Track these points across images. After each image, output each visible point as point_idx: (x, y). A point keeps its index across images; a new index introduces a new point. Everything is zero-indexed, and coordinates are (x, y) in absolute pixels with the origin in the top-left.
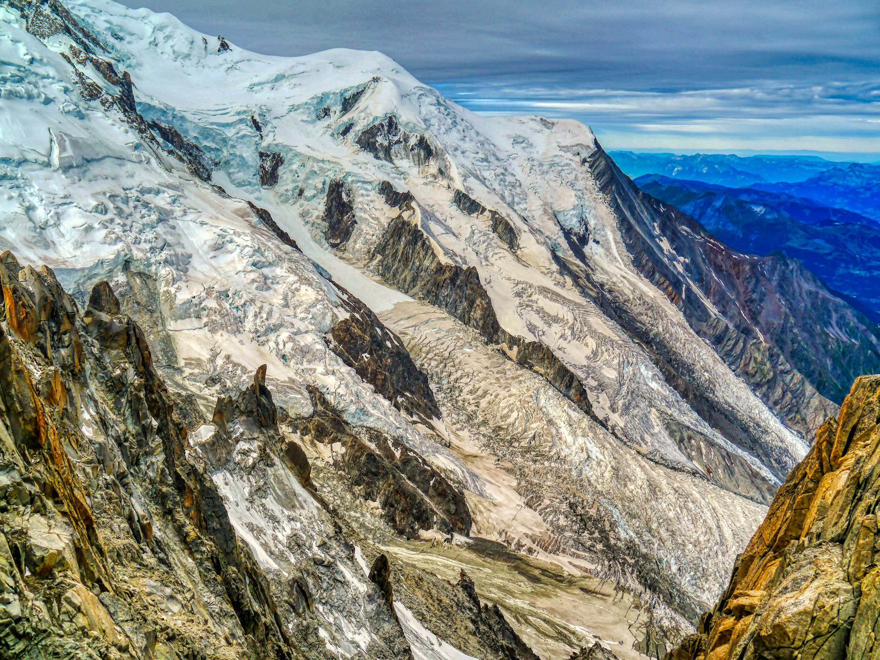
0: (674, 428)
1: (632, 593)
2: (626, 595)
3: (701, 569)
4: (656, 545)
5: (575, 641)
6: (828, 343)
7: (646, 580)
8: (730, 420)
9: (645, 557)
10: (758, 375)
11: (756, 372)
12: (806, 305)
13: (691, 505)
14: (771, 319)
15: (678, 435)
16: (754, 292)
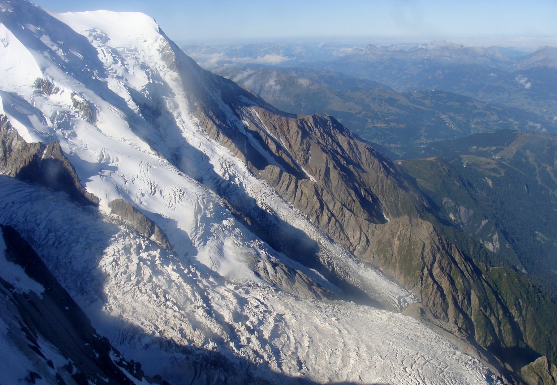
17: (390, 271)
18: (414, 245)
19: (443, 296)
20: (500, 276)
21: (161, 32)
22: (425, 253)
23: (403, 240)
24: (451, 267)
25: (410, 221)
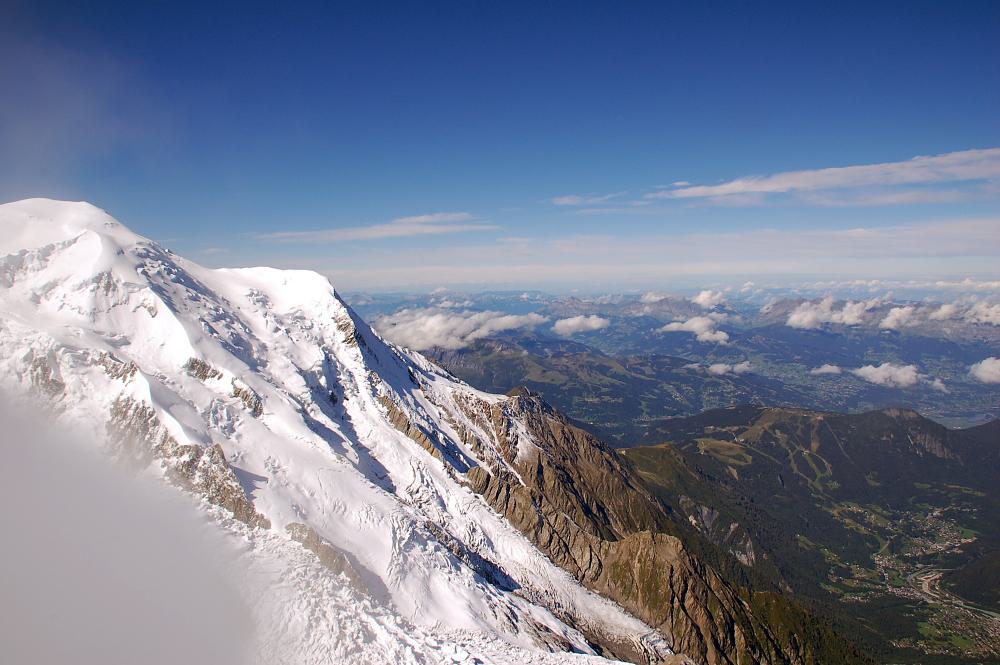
16: (508, 435)
17: (631, 603)
19: (700, 635)
20: (767, 604)
21: (337, 296)
22: (674, 579)
24: (707, 595)
25: (653, 537)
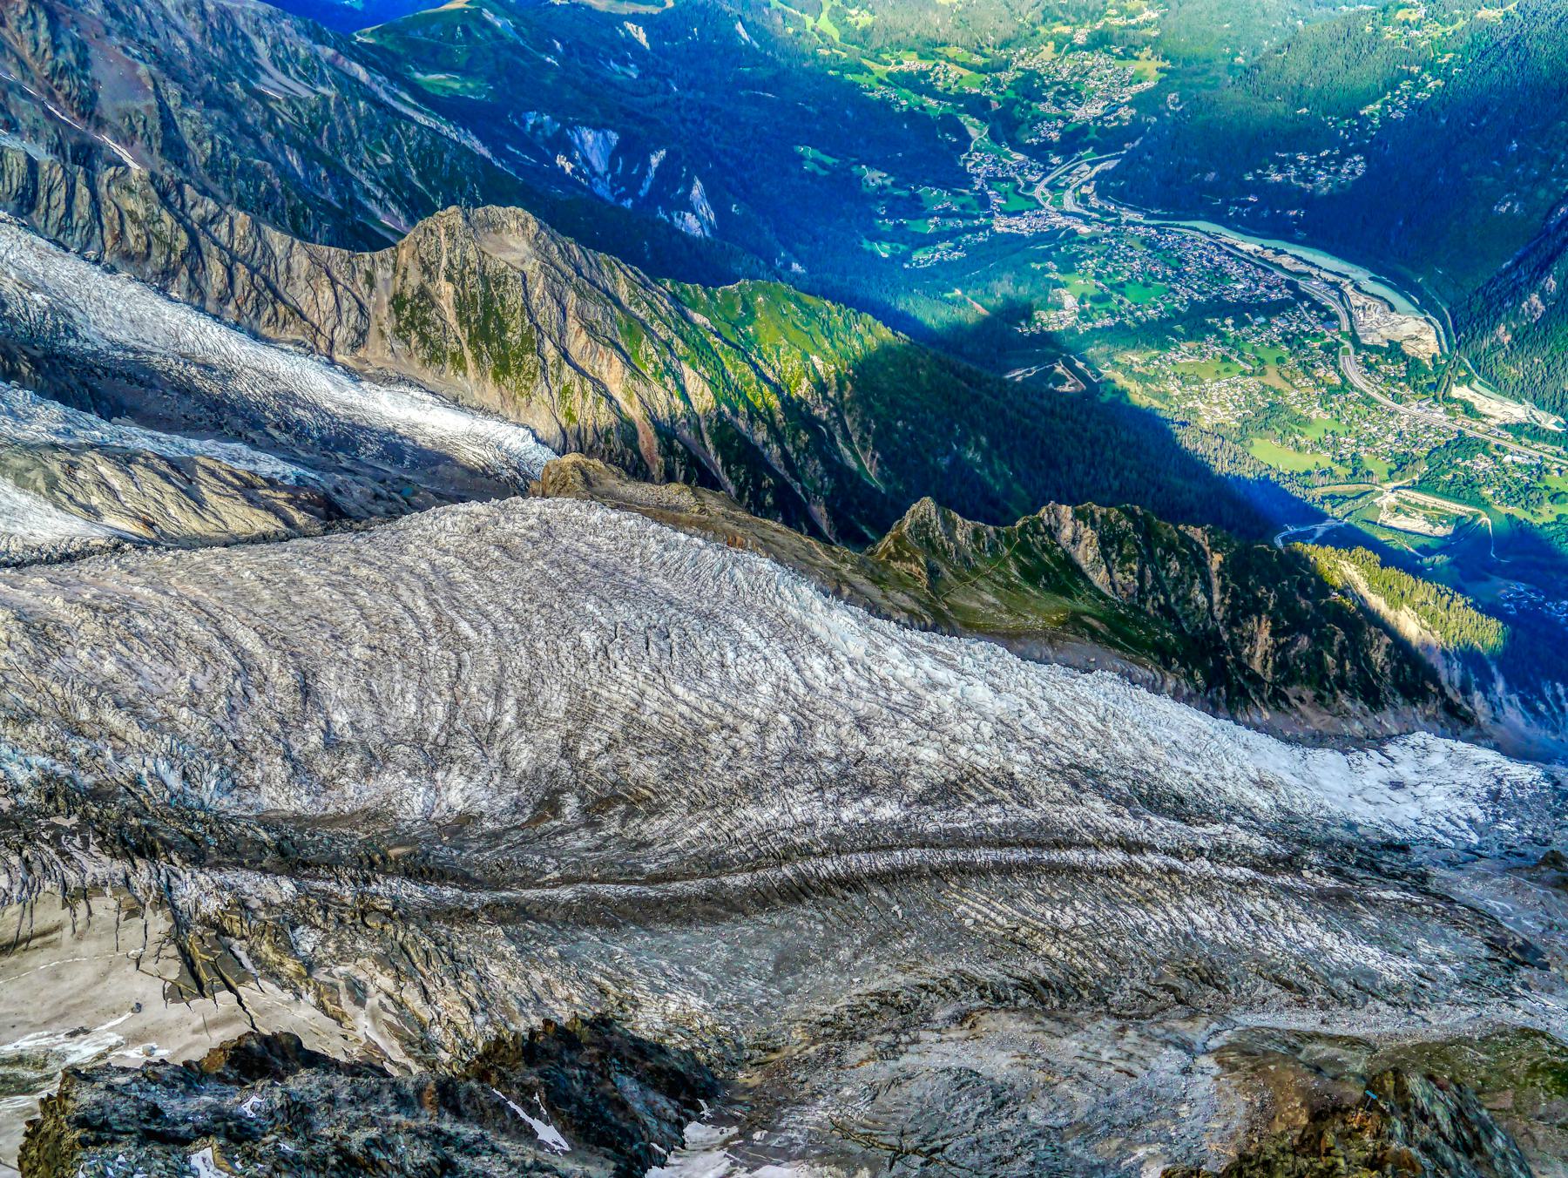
0: (19, 463)
1: (108, 891)
2: (95, 903)
3: (229, 747)
4: (109, 752)
5: (29, 1074)
6: (273, 116)
7: (124, 842)
8: (141, 383)
9: (96, 794)
10: (155, 252)
11: (149, 246)
12: (190, 43)
13: (142, 622)
14: (122, 104)
15: (36, 475)
18: (497, 285)
23: (462, 278)
